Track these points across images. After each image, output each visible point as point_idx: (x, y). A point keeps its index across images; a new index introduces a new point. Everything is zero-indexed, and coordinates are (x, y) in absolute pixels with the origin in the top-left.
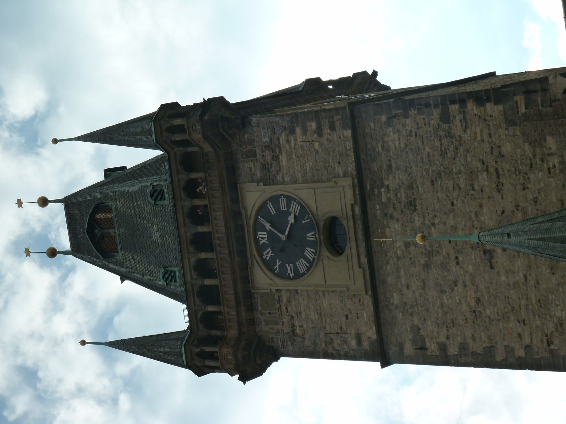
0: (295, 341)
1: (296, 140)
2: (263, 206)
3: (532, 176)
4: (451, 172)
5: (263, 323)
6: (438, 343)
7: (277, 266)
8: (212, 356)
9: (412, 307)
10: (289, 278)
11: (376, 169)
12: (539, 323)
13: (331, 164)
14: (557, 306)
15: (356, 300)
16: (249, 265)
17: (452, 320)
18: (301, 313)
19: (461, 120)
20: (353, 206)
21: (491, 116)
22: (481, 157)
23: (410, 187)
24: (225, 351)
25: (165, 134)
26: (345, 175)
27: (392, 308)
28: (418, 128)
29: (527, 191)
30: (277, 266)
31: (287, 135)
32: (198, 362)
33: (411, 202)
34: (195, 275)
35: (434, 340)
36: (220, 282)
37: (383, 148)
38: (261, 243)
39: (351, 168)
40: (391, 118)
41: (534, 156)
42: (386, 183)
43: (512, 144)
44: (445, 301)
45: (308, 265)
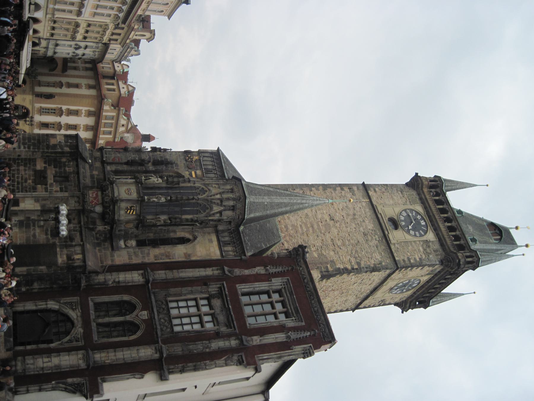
4: (352, 245)
8: (431, 181)
20: (388, 233)
23: (367, 240)
32: (437, 179)
39: (392, 247)
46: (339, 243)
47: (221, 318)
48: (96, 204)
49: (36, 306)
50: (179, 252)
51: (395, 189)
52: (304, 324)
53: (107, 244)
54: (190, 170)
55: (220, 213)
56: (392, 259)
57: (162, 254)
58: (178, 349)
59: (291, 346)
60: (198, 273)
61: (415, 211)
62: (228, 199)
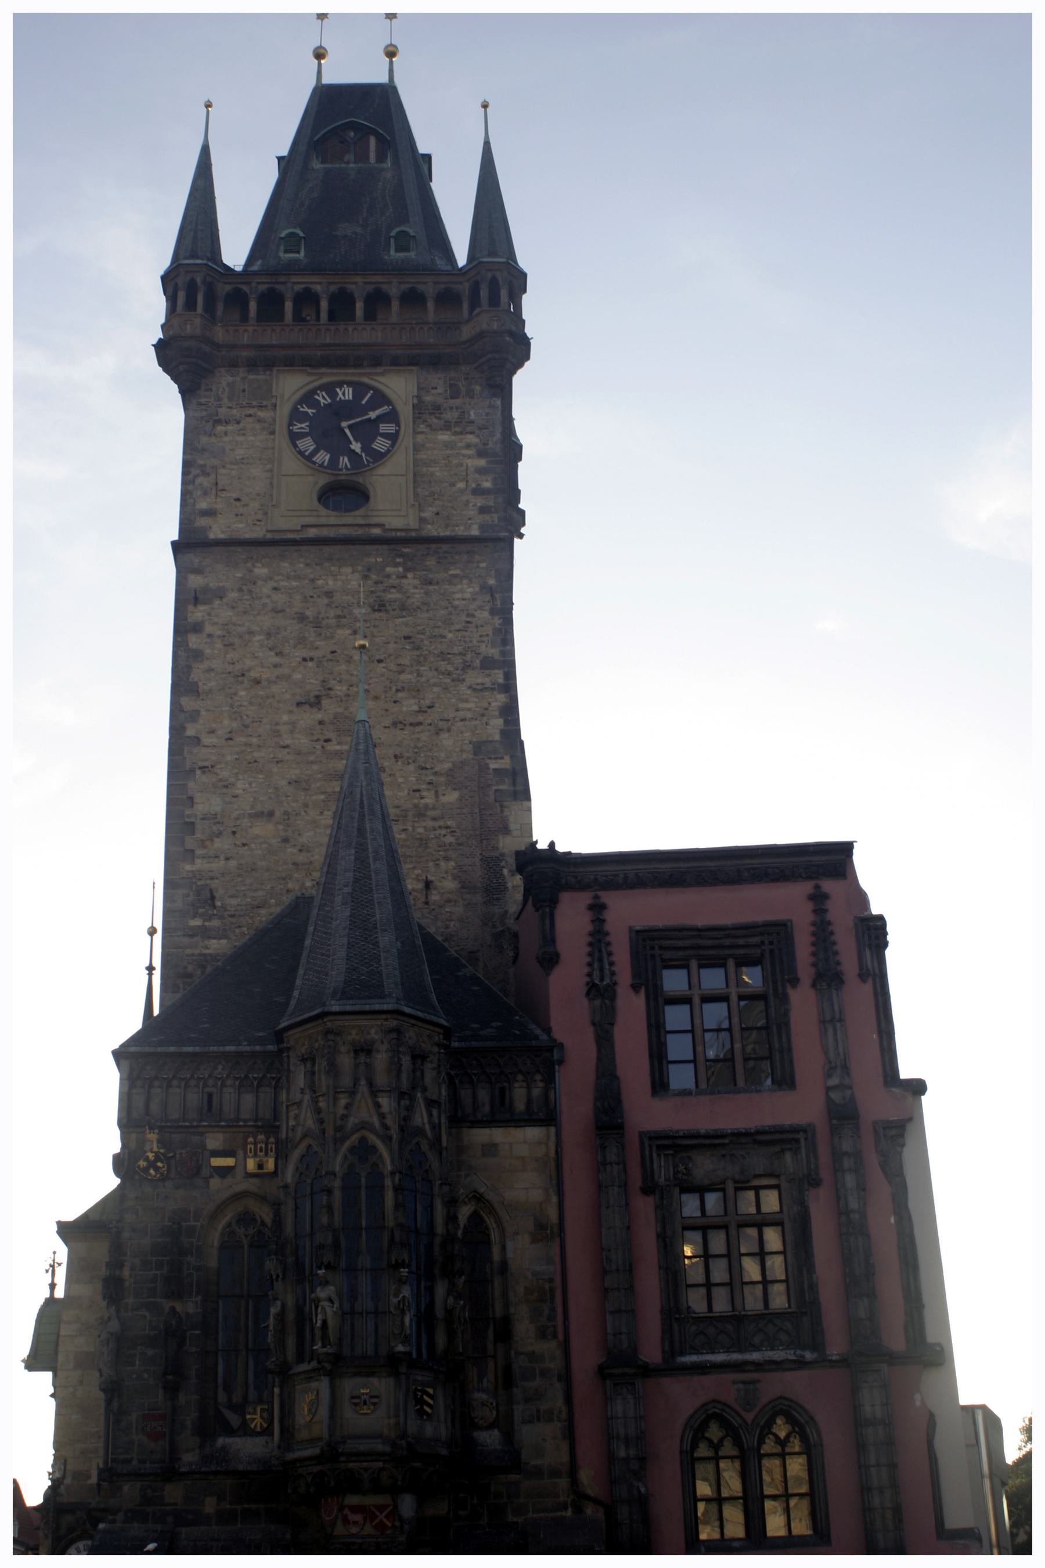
0: (207, 421)
1: (469, 457)
3: (411, 768)
5: (230, 379)
6: (203, 622)
7: (306, 409)
8: (190, 305)
9: (250, 592)
10: (291, 424)
11: (428, 563)
12: (229, 758)
13: (437, 502)
14: (250, 784)
15: (260, 516)
16: (308, 369)
17: (232, 644)
18: (243, 435)
19: (483, 684)
21: (487, 724)
22: (437, 705)
24: (198, 321)
25: (489, 275)
26: (422, 520)
27: (249, 565)
28: (477, 627)
29: (393, 759)
30: (306, 409)
31: (476, 446)
32: (182, 280)
33: (384, 605)
34: (298, 288)
35: (207, 617)
36: (288, 325)
37: (455, 576)
38: (338, 390)
39: (432, 530)
40: (491, 591)
41: (436, 773)
42: (410, 575)
44: (258, 638)
45: (307, 453)
46: (410, 705)
51: (204, 439)
54: (205, 1172)
55: (430, 1103)
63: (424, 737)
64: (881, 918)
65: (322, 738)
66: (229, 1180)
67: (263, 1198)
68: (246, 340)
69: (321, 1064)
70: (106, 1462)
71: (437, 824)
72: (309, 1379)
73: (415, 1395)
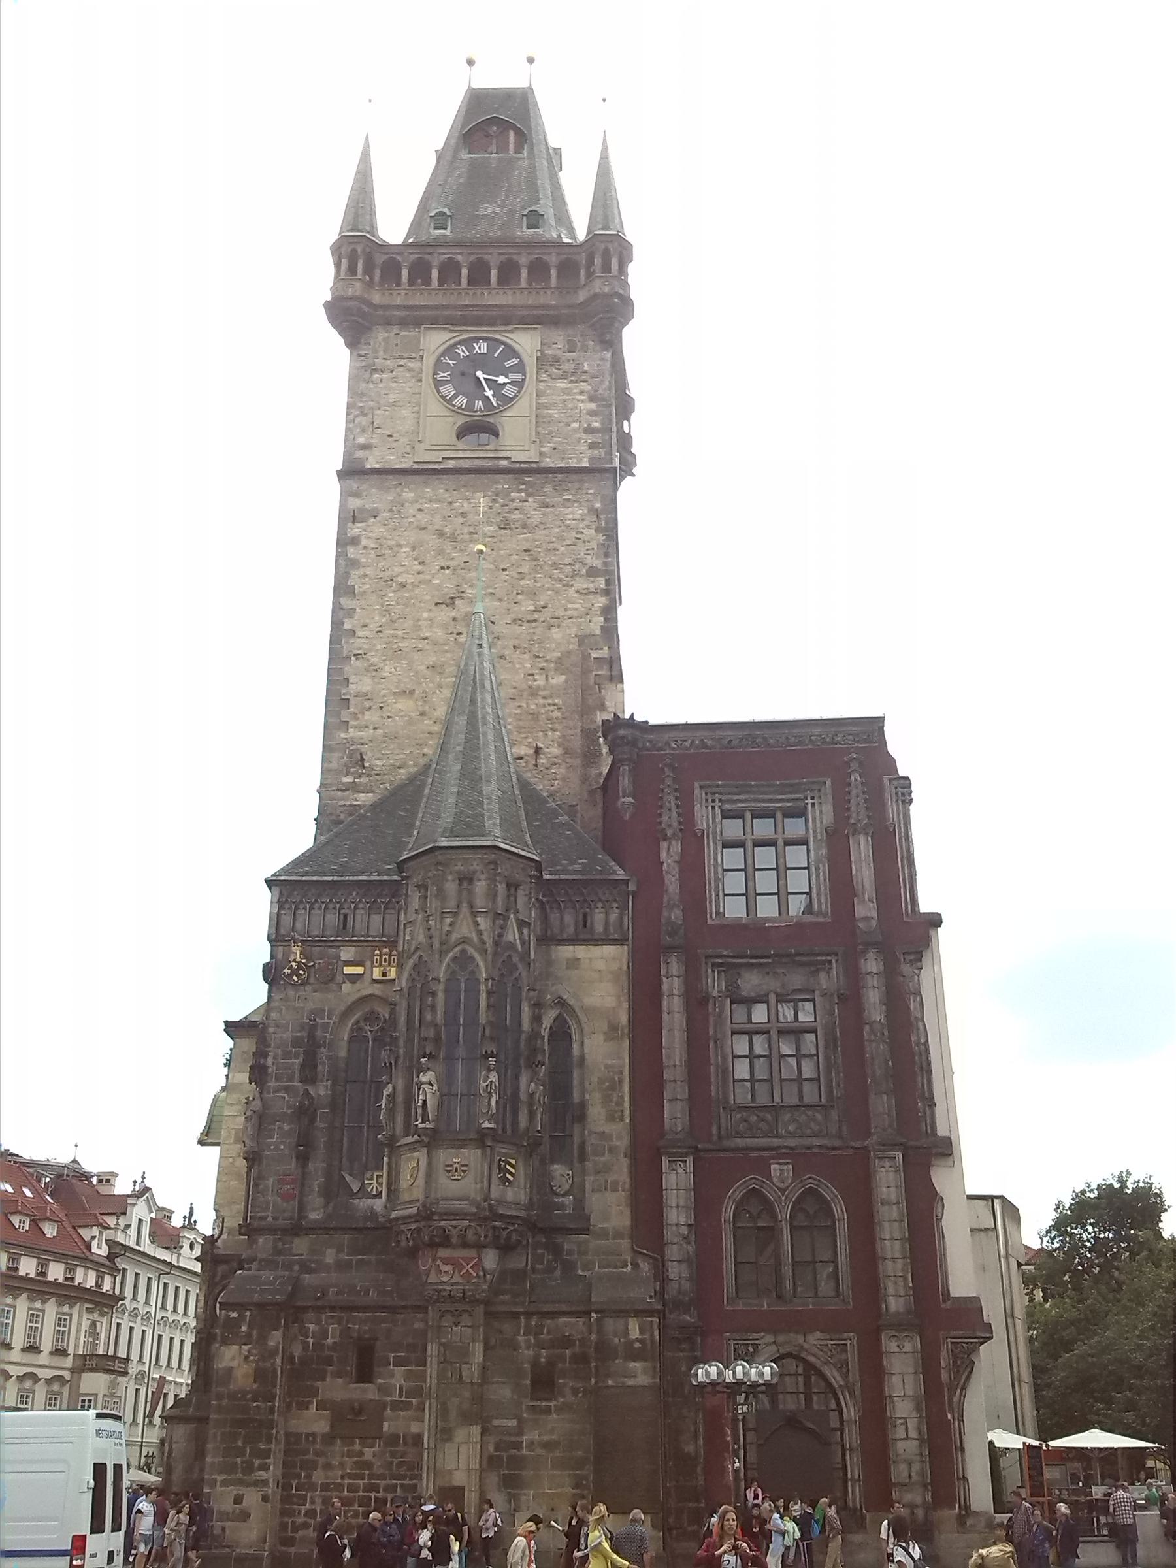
1: (583, 402)
2: (513, 353)
3: (526, 656)
8: (352, 270)
12: (379, 647)
15: (408, 449)
23: (524, 526)
25: (603, 246)
31: (588, 392)
39: (549, 463)
40: (597, 513)
41: (547, 661)
42: (530, 499)
43: (561, 639)
47: (796, 979)
48: (478, 1265)
49: (851, 1450)
50: (601, 1053)
52: (829, 782)
53: (569, 1243)
55: (522, 924)
56: (585, 477)
57: (607, 1099)
58: (882, 1105)
59: (887, 827)
60: (677, 1015)
61: (443, 354)
62: (492, 895)
63: (538, 631)
64: (907, 778)
65: (456, 631)
66: (358, 985)
67: (383, 1000)
68: (398, 301)
69: (432, 890)
70: (245, 1219)
71: (546, 702)
72: (414, 1150)
73: (500, 1165)
